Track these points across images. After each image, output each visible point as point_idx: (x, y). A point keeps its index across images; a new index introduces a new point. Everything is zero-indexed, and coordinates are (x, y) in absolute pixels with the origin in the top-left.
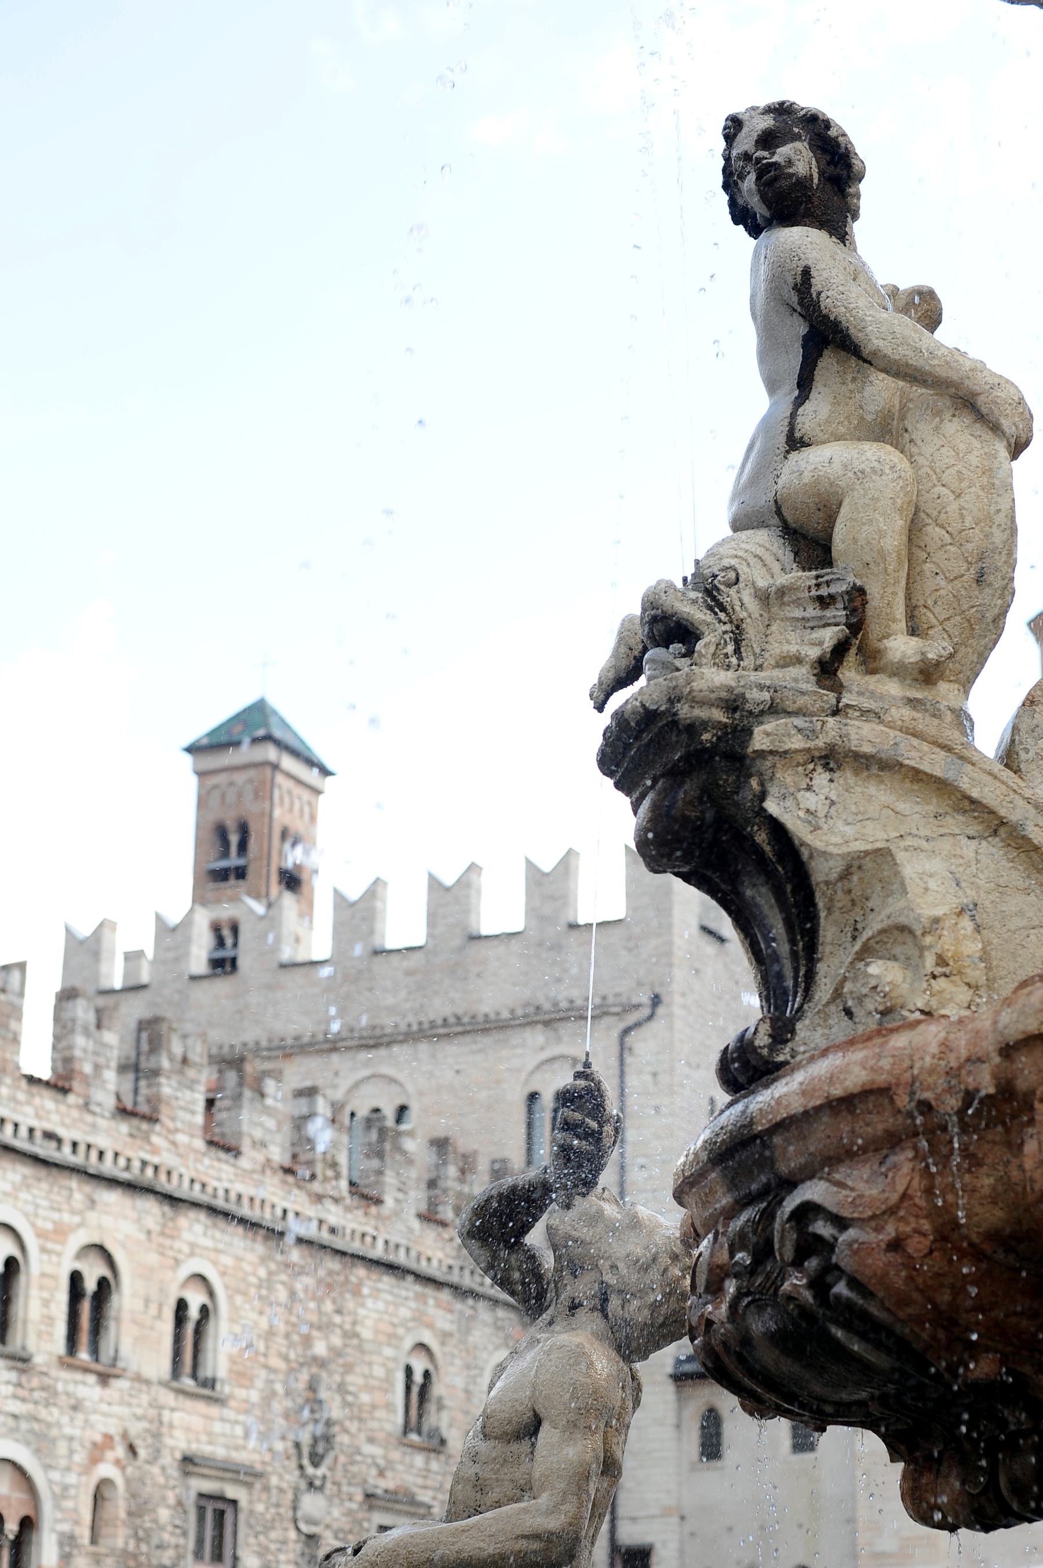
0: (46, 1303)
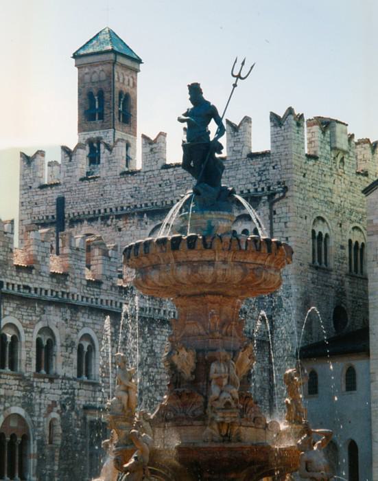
0: (28, 353)
